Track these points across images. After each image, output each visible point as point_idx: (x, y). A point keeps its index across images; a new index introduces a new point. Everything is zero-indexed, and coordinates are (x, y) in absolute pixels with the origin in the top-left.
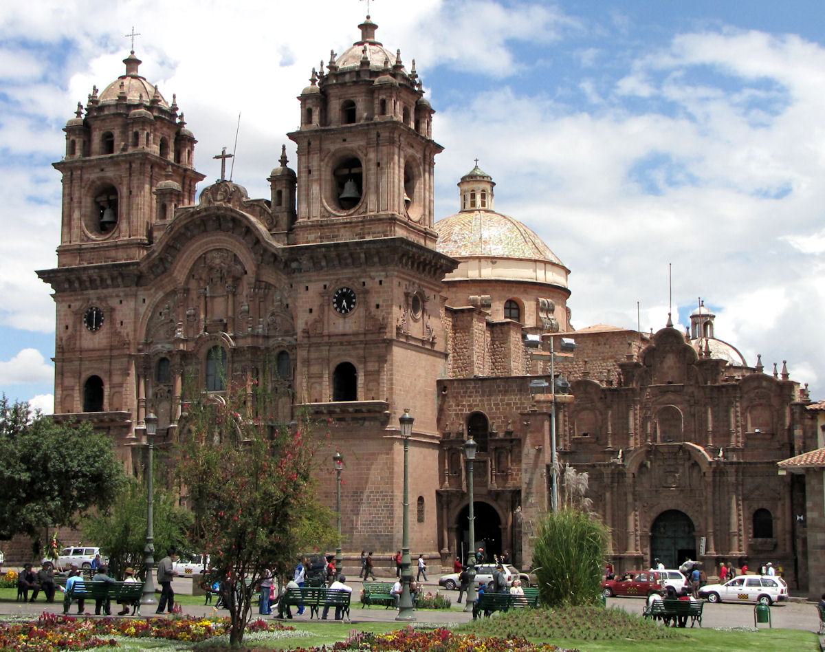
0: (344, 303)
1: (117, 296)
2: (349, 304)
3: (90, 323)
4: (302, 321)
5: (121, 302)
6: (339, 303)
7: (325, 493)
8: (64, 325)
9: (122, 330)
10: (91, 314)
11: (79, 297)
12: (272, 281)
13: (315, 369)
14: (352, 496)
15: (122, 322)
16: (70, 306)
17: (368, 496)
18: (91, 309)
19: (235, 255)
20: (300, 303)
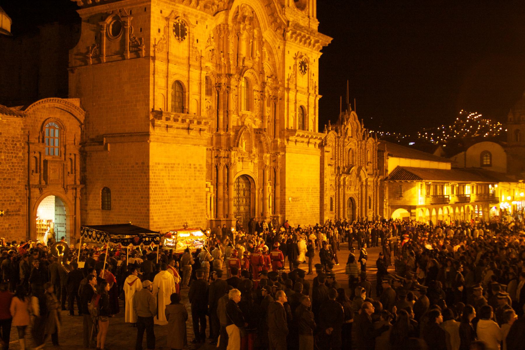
0: (303, 68)
1: (196, 16)
2: (305, 69)
3: (177, 35)
4: (288, 72)
5: (197, 23)
6: (301, 66)
7: (297, 188)
8: (158, 28)
9: (198, 47)
10: (177, 24)
11: (171, 6)
12: (268, 40)
13: (292, 107)
14: (307, 190)
15: (197, 40)
16: (161, 12)
17: (312, 190)
18: (179, 20)
19: (255, 14)
20: (286, 62)
